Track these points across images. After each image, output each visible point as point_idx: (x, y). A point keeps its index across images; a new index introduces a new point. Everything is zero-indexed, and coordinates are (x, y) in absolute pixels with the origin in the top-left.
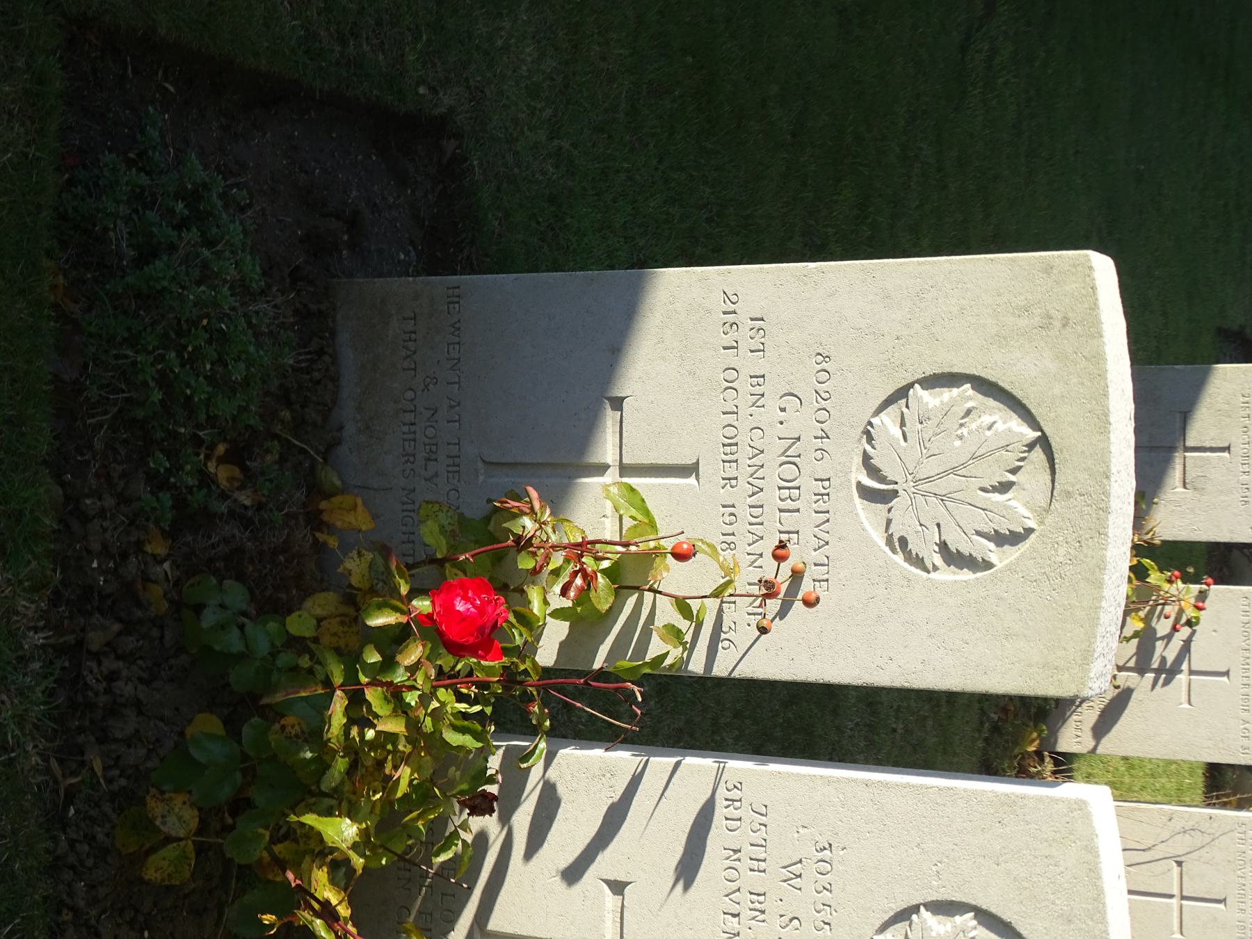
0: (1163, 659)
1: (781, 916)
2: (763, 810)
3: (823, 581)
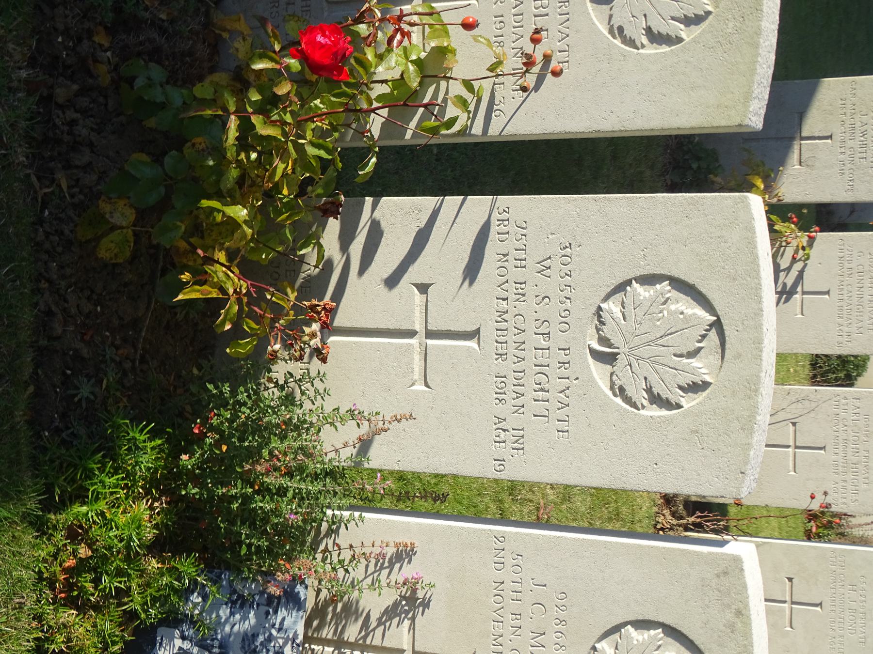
0: (785, 285)
1: (537, 296)
2: (524, 225)
3: (565, 62)
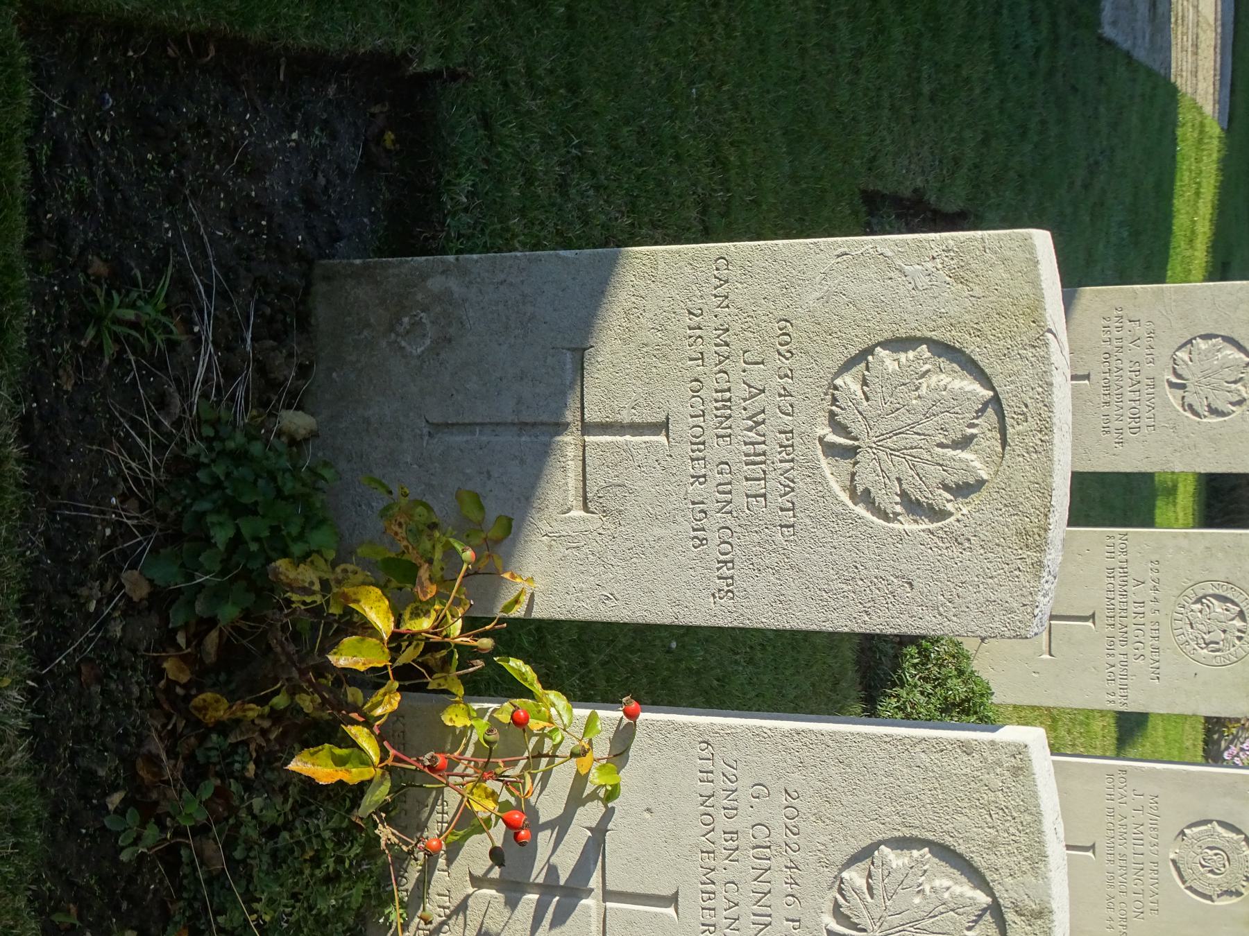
0: (552, 870)
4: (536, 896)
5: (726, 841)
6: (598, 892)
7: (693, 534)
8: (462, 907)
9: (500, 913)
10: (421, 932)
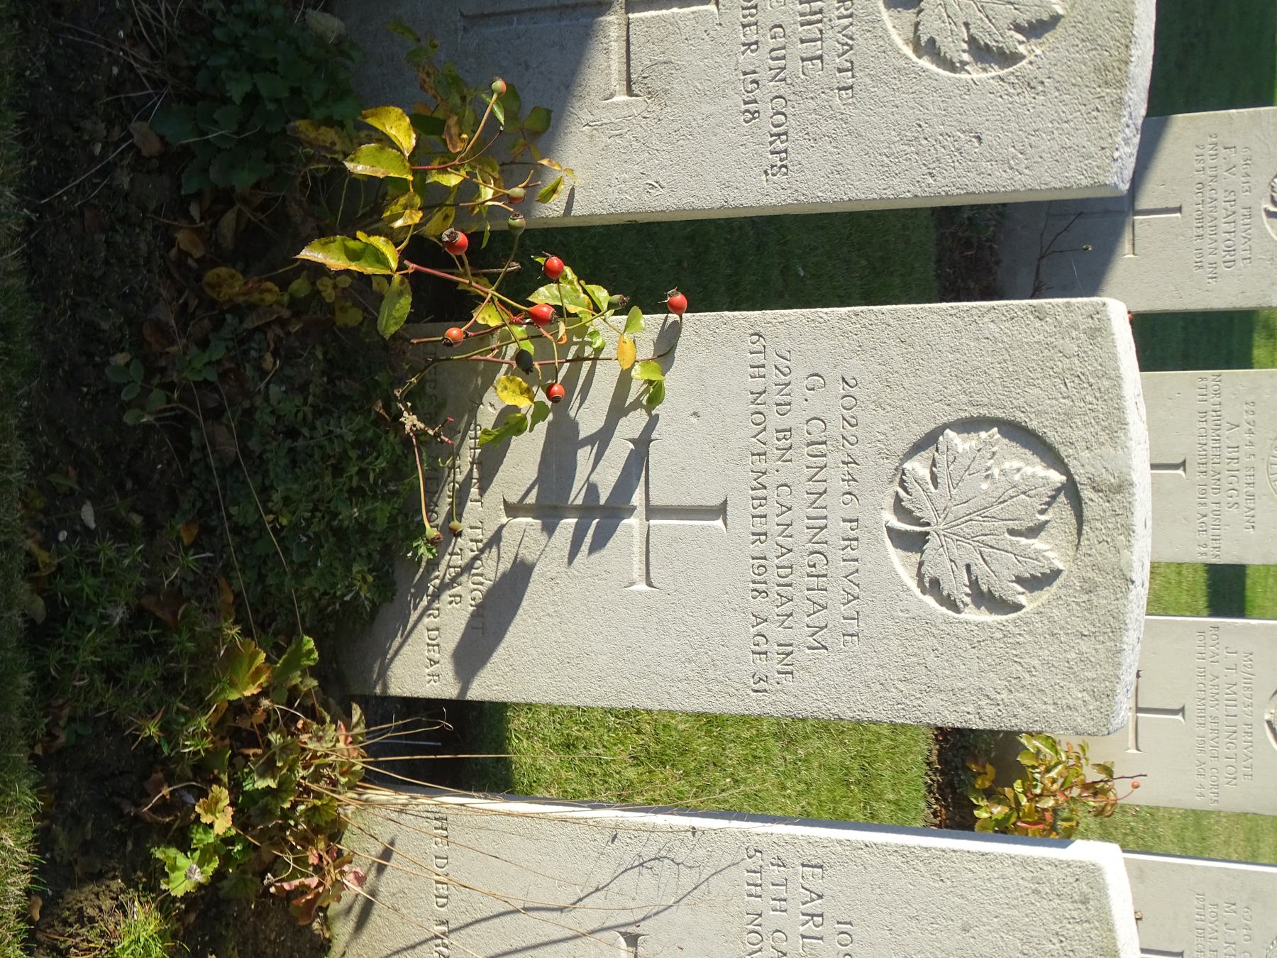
0: (592, 490)
4: (576, 520)
5: (778, 440)
6: (641, 510)
7: (744, 107)
8: (496, 539)
9: (536, 541)
10: (452, 570)
